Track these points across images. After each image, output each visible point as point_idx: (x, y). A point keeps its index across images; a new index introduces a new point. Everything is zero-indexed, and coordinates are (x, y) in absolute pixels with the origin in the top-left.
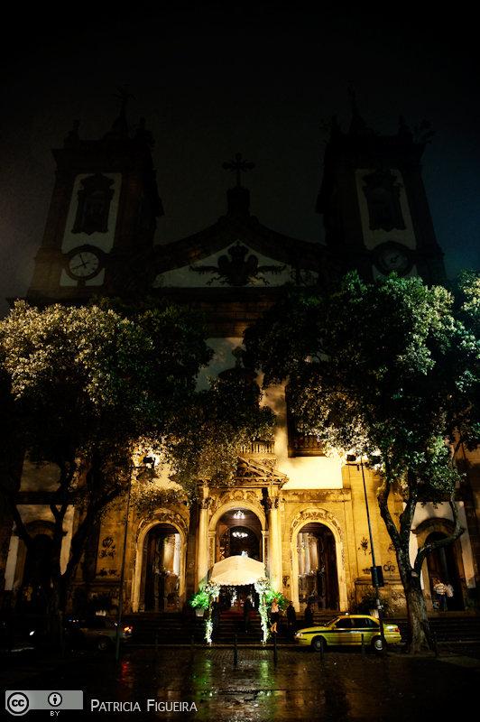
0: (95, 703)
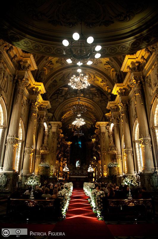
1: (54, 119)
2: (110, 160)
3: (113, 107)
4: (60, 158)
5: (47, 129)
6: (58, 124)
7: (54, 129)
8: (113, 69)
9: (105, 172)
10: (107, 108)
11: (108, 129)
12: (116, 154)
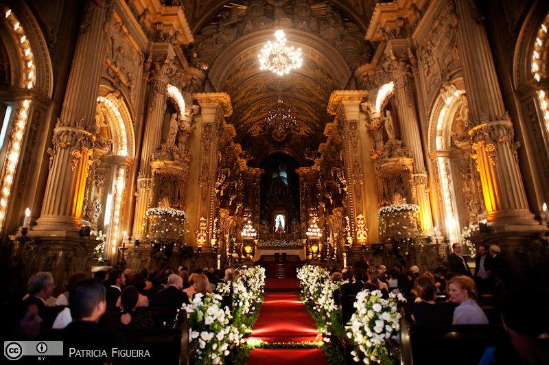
0: (72, 351)
1: (207, 87)
2: (375, 200)
3: (393, 26)
4: (234, 206)
5: (188, 114)
6: (222, 104)
7: (208, 116)
9: (362, 235)
10: (368, 36)
11: (367, 113)
12: (408, 170)
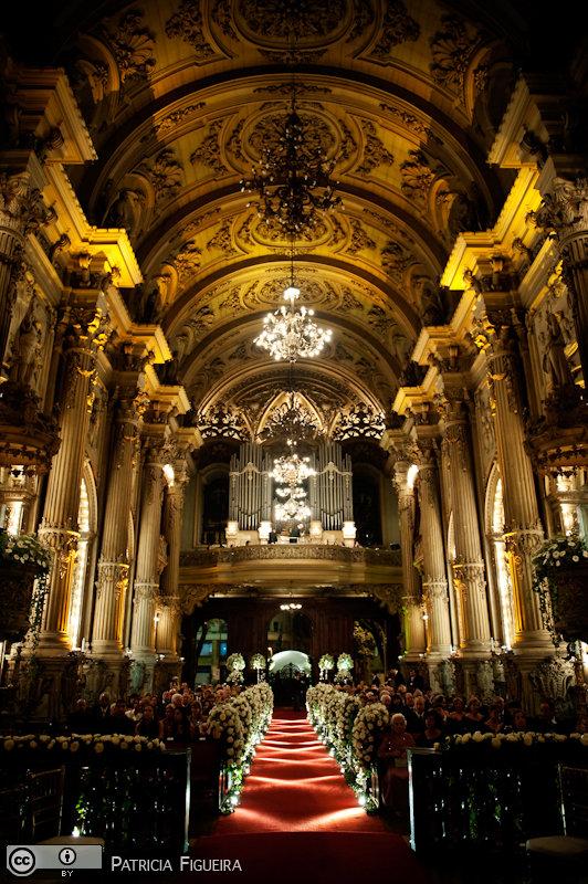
8: (441, 181)
